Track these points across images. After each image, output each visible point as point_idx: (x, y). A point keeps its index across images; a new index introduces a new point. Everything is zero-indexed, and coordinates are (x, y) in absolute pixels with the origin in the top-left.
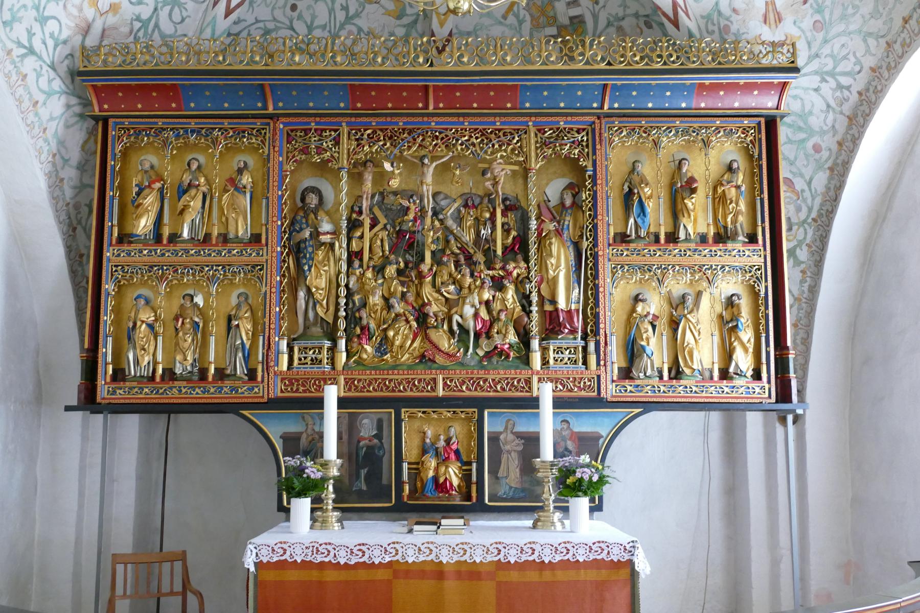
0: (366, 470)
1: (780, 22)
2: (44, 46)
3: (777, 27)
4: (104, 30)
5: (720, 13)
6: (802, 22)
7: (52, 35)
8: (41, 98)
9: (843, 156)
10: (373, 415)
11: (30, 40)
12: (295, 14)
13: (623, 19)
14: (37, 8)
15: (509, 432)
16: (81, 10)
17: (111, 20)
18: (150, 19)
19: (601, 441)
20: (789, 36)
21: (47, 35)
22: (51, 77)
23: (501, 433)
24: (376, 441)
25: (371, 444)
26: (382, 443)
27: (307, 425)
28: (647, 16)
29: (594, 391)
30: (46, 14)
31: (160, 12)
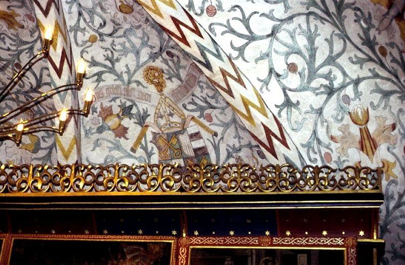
1: (376, 149)
3: (373, 153)
5: (319, 142)
6: (394, 148)
13: (240, 150)
20: (385, 162)
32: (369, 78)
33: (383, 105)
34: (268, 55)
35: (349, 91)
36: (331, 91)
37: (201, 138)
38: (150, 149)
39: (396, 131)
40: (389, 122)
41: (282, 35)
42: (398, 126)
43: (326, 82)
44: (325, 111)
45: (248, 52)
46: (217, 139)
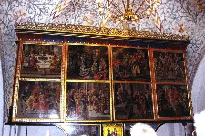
2: (6, 22)
4: (21, 19)
5: (169, 29)
6: (188, 32)
7: (9, 19)
8: (3, 35)
9: (197, 62)
10: (95, 126)
11: (3, 19)
12: (67, 21)
13: (146, 29)
14: (6, 11)
16: (16, 13)
17: (23, 17)
18: (33, 18)
21: (8, 19)
22: (7, 30)
24: (96, 133)
25: (94, 134)
26: (97, 133)
28: (152, 29)
30: (8, 13)
31: (36, 17)
32: (185, 16)
33: (187, 23)
34: (163, 8)
35: (179, 19)
36: (175, 18)
37: (135, 25)
38: (121, 27)
39: (190, 28)
40: (188, 26)
41: (168, 4)
42: (190, 28)
43: (174, 16)
44: (172, 22)
45: (160, 7)
46: (139, 26)
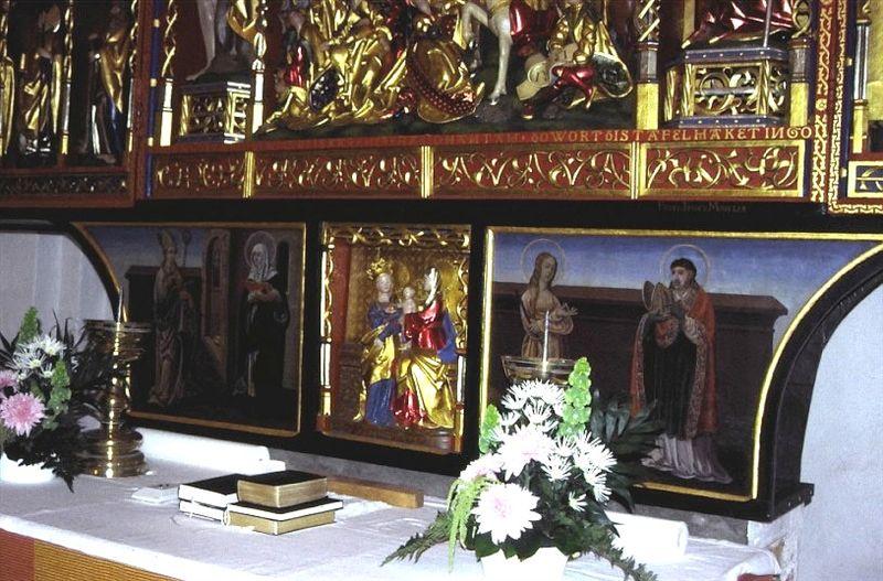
0: (256, 353)
15: (542, 285)
19: (780, 321)
23: (522, 287)
24: (275, 292)
26: (284, 296)
27: (165, 252)
29: (794, 187)
